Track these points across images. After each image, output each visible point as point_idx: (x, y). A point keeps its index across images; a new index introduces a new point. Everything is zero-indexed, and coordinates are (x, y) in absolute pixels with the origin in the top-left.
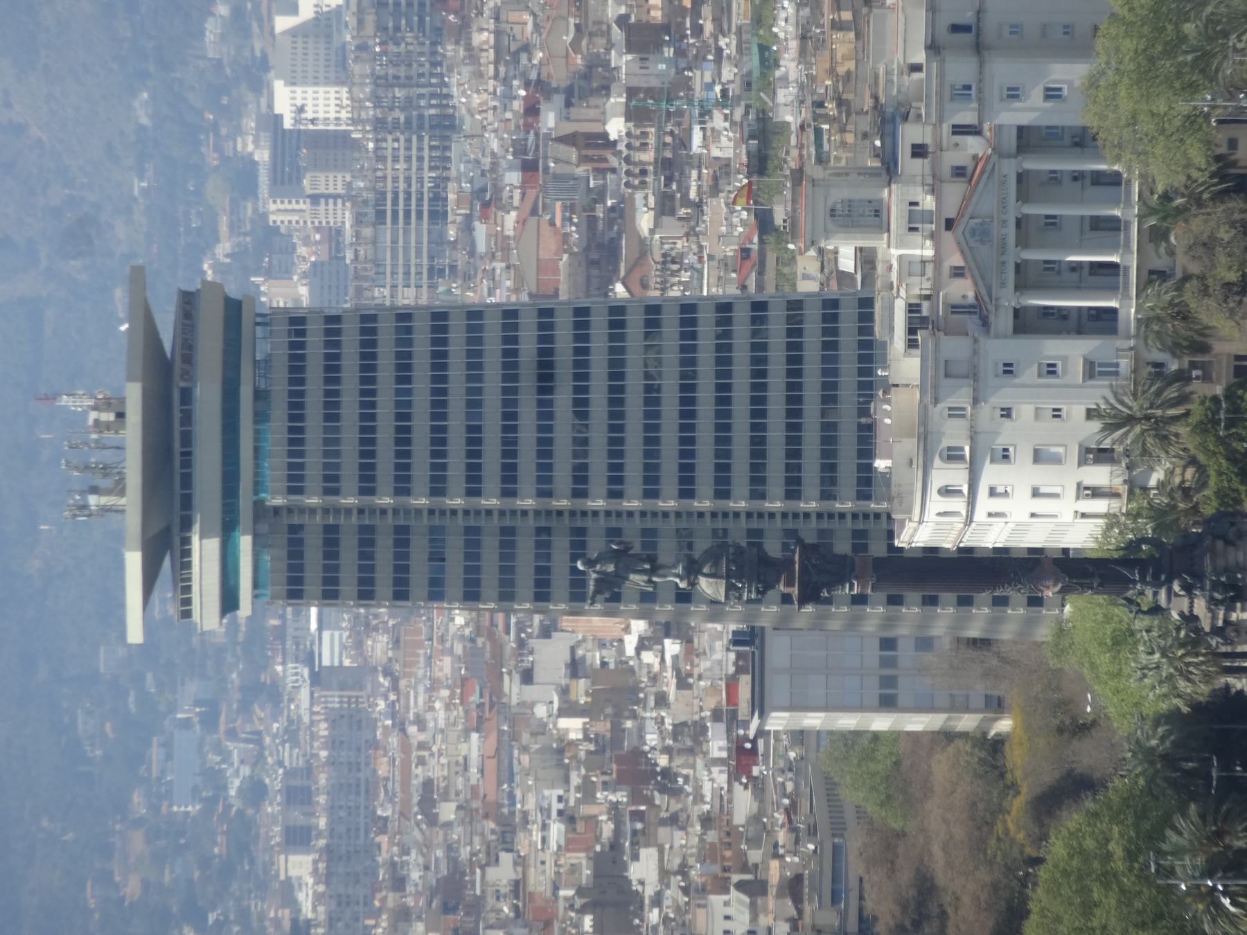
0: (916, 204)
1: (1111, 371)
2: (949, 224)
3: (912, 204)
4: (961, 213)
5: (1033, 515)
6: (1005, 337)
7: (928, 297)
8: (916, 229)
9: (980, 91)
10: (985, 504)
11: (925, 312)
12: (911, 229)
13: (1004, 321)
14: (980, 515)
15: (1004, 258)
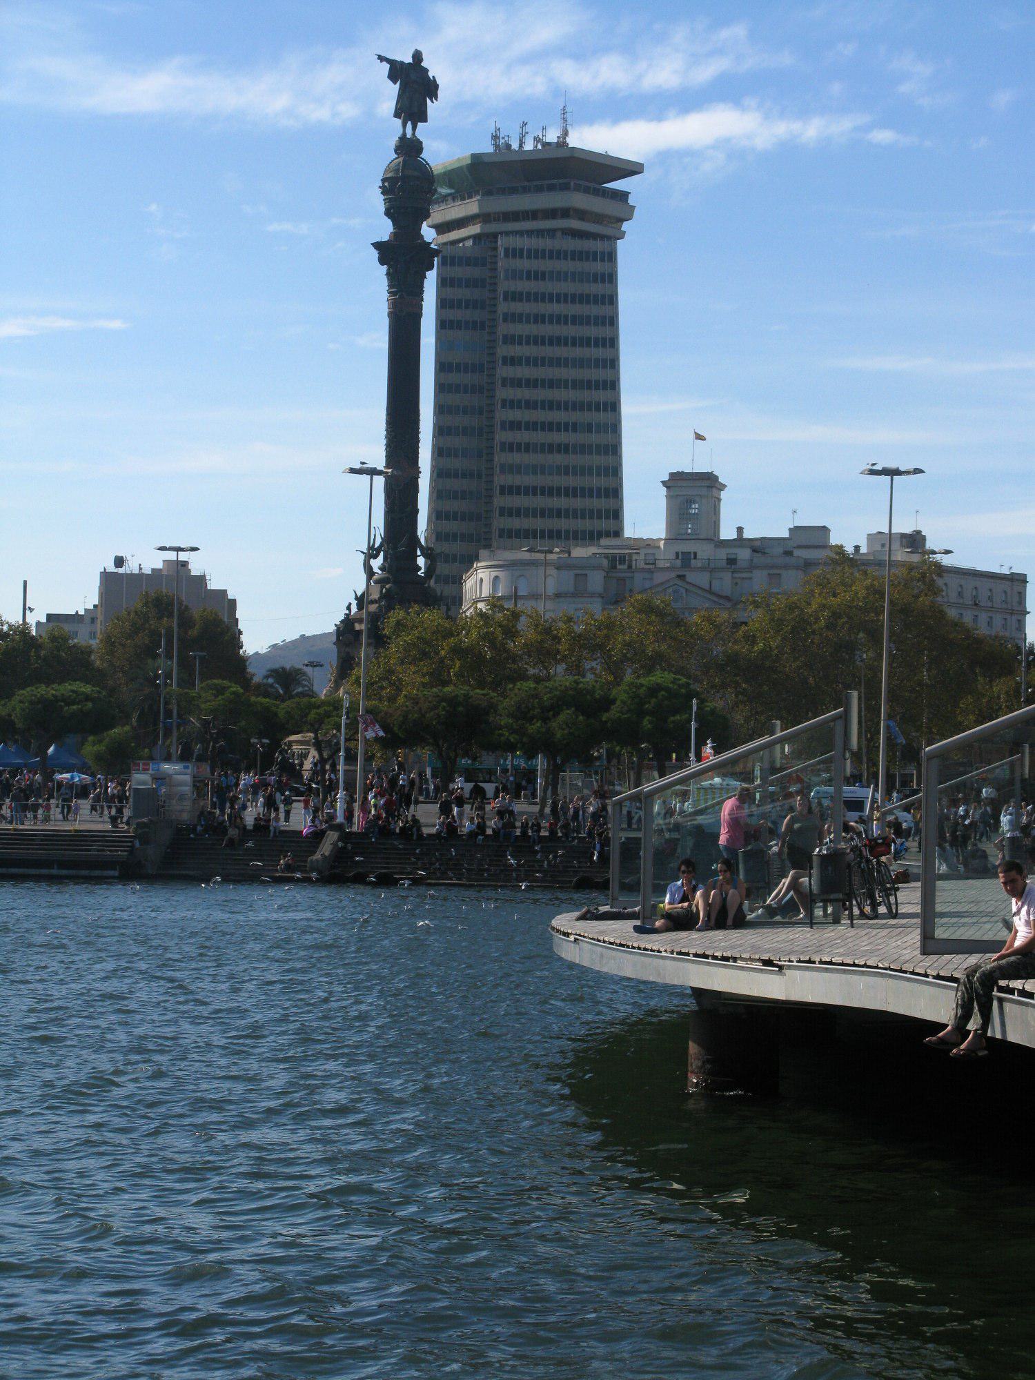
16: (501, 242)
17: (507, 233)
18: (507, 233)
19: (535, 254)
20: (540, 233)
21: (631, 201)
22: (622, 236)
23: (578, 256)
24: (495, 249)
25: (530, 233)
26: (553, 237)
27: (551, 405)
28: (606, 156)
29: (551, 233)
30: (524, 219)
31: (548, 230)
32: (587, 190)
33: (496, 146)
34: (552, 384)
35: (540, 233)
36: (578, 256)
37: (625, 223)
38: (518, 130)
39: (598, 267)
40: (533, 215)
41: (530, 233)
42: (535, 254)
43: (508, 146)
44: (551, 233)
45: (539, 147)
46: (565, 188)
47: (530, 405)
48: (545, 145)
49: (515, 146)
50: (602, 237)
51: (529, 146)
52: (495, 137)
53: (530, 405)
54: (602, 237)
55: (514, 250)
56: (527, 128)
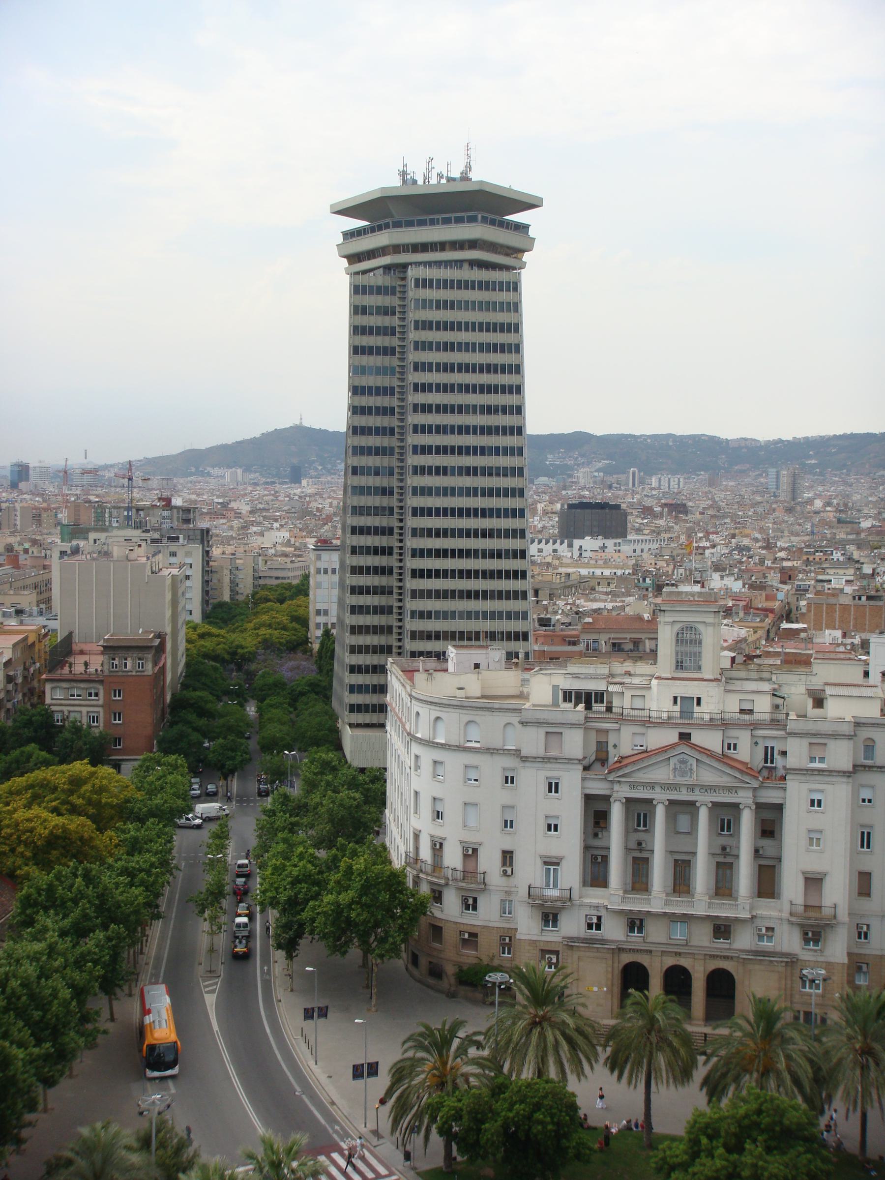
0: (699, 703)
1: (551, 879)
2: (685, 737)
3: (699, 700)
4: (695, 747)
5: (416, 793)
6: (583, 788)
7: (609, 709)
8: (675, 702)
9: (820, 771)
10: (427, 756)
11: (596, 707)
12: (675, 698)
13: (597, 788)
14: (416, 749)
15: (658, 789)
16: (411, 272)
17: (418, 264)
18: (418, 264)
19: (445, 284)
20: (447, 264)
21: (531, 233)
22: (523, 266)
23: (485, 286)
24: (404, 279)
25: (439, 264)
26: (461, 267)
27: (463, 430)
28: (510, 190)
29: (459, 263)
30: (432, 250)
31: (456, 261)
32: (493, 223)
33: (404, 182)
34: (460, 409)
35: (447, 264)
36: (485, 286)
37: (526, 253)
38: (425, 165)
39: (504, 296)
40: (442, 246)
41: (439, 264)
42: (445, 284)
43: (415, 182)
44: (459, 263)
45: (444, 181)
46: (472, 219)
47: (440, 429)
48: (450, 180)
49: (420, 182)
50: (508, 268)
51: (434, 181)
52: (403, 174)
53: (440, 429)
54: (508, 268)
55: (424, 280)
56: (433, 164)
